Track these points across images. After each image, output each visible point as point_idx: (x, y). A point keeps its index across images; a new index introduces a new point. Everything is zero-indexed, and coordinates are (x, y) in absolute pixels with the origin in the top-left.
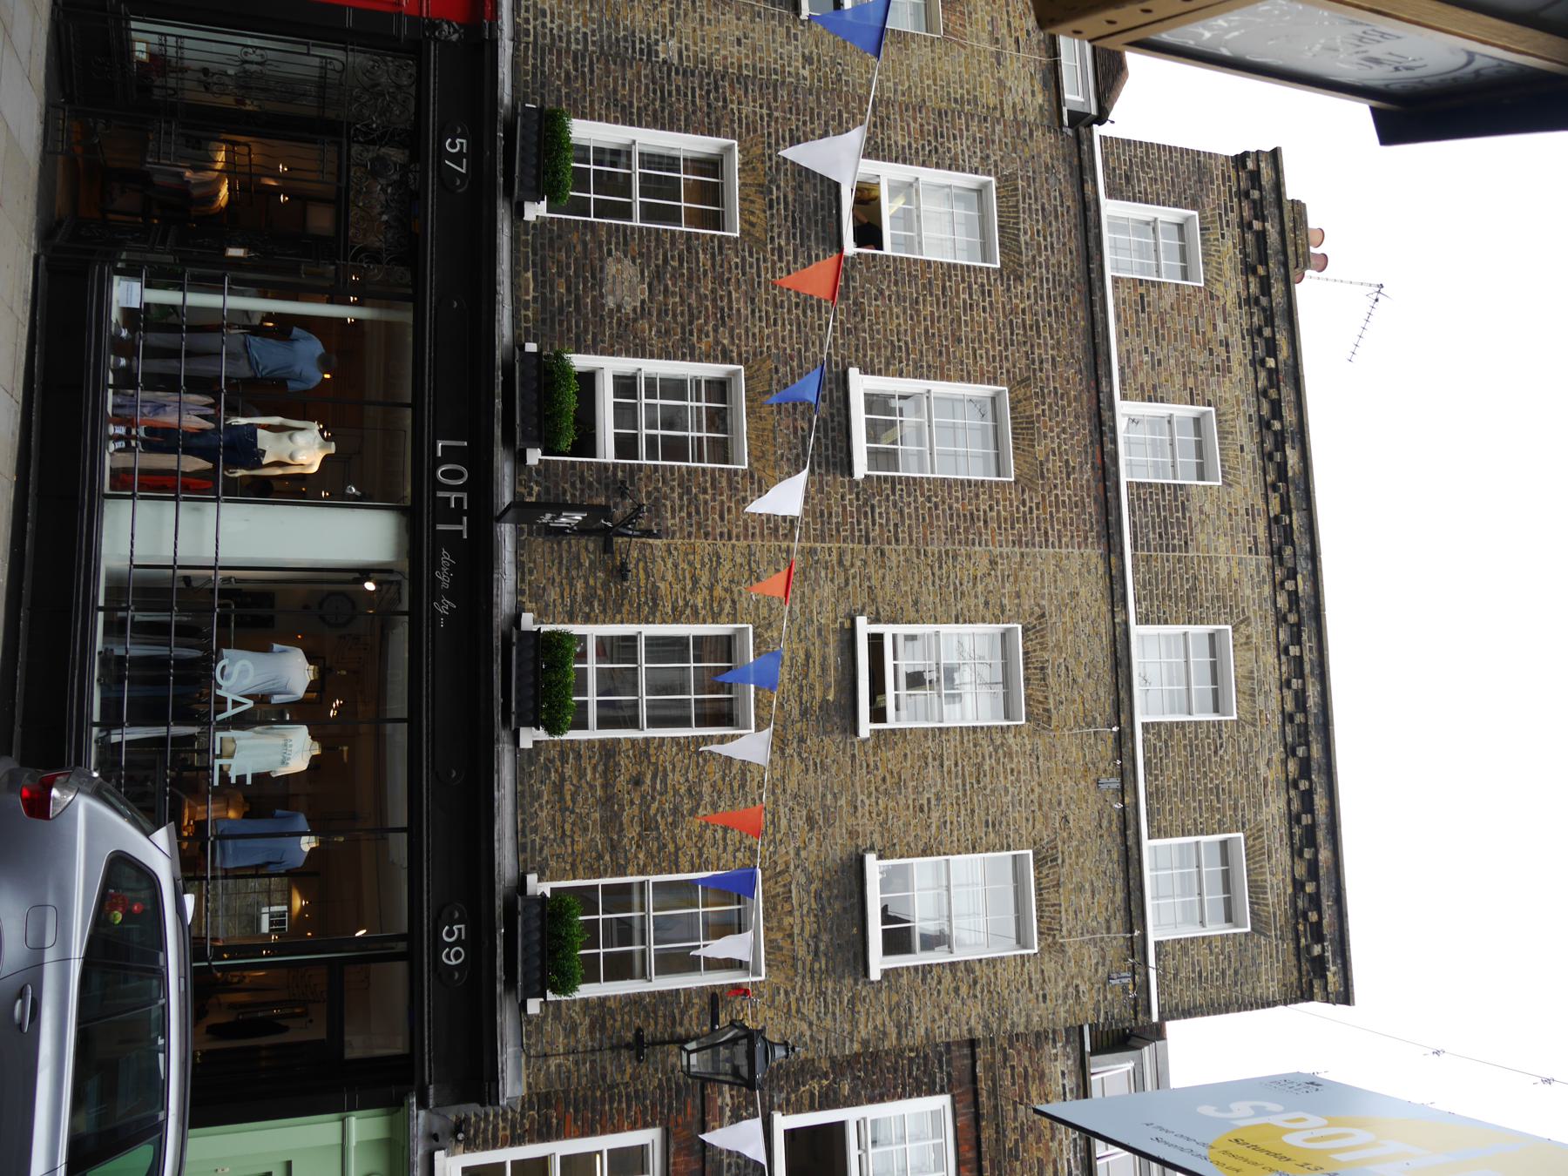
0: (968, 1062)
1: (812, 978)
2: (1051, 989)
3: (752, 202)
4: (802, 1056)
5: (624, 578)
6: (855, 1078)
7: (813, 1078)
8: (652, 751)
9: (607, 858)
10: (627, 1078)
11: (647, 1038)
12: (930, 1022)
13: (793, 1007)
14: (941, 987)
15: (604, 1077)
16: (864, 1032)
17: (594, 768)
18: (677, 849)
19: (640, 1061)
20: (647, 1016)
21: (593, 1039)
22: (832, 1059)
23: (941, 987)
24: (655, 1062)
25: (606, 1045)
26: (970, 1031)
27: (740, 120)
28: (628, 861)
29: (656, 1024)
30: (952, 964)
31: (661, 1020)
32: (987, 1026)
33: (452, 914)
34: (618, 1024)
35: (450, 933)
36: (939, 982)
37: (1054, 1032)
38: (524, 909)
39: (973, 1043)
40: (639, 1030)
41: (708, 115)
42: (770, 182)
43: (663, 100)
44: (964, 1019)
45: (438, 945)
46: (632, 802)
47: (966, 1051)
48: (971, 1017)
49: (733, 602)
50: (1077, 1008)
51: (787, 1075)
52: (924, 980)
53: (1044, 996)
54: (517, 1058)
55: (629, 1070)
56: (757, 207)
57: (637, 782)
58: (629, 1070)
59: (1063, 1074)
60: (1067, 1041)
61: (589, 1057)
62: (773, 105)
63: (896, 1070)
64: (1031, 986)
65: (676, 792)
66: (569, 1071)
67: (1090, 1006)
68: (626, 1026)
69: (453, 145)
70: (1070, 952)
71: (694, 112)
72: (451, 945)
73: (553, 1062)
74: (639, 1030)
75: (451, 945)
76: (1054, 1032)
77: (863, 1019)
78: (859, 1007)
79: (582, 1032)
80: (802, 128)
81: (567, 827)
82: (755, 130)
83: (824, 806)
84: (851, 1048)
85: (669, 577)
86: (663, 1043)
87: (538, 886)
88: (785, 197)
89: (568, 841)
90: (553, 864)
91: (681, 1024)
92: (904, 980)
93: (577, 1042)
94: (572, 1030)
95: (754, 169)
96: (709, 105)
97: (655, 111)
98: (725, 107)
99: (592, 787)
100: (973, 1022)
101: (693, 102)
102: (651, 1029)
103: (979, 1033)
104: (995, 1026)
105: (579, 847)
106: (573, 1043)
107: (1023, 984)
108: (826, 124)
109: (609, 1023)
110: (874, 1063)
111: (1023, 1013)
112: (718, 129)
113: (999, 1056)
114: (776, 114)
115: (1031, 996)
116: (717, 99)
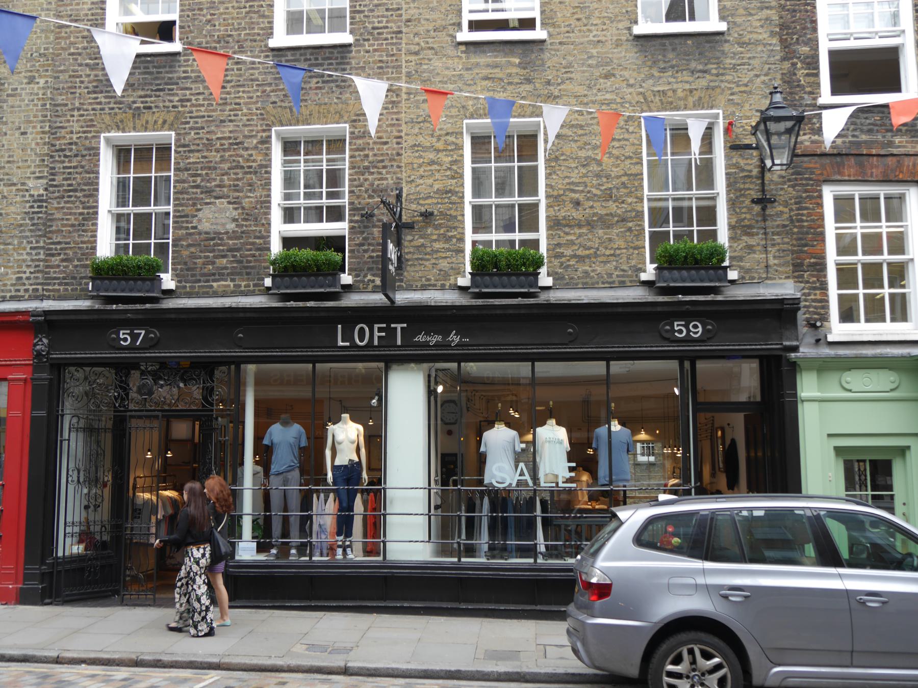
1: (723, 75)
3: (147, 122)
5: (431, 214)
7: (795, 74)
8: (555, 193)
9: (630, 224)
10: (786, 210)
11: (756, 195)
13: (743, 89)
15: (784, 226)
17: (567, 234)
18: (626, 174)
19: (775, 201)
20: (743, 195)
21: (757, 234)
22: (784, 59)
24: (776, 190)
25: (762, 224)
27: (84, 132)
28: (634, 210)
29: (750, 189)
31: (747, 186)
33: (667, 331)
34: (748, 216)
35: (680, 332)
38: (665, 281)
40: (753, 201)
41: (83, 156)
42: (130, 108)
43: (75, 190)
45: (688, 340)
46: (592, 207)
49: (447, 134)
51: (791, 93)
54: (767, 286)
55: (781, 208)
56: (151, 119)
57: (577, 203)
58: (781, 208)
61: (770, 236)
62: (70, 106)
65: (585, 176)
66: (779, 250)
68: (750, 210)
69: (125, 340)
71: (83, 167)
72: (689, 331)
73: (772, 261)
74: (753, 201)
75: (689, 331)
79: (752, 241)
80: (86, 84)
81: (608, 252)
82: (92, 120)
83: (597, 66)
85: (430, 181)
86: (763, 184)
87: (649, 272)
88: (141, 97)
89: (618, 252)
90: (633, 263)
91: (751, 171)
93: (758, 245)
94: (750, 248)
95: (122, 121)
96: (76, 156)
97: (85, 196)
98: (76, 144)
99: (580, 235)
101: (75, 167)
102: (752, 192)
105: (622, 244)
106: (759, 248)
108: (80, 65)
109: (747, 222)
112: (93, 148)
114: (77, 105)
116: (71, 150)
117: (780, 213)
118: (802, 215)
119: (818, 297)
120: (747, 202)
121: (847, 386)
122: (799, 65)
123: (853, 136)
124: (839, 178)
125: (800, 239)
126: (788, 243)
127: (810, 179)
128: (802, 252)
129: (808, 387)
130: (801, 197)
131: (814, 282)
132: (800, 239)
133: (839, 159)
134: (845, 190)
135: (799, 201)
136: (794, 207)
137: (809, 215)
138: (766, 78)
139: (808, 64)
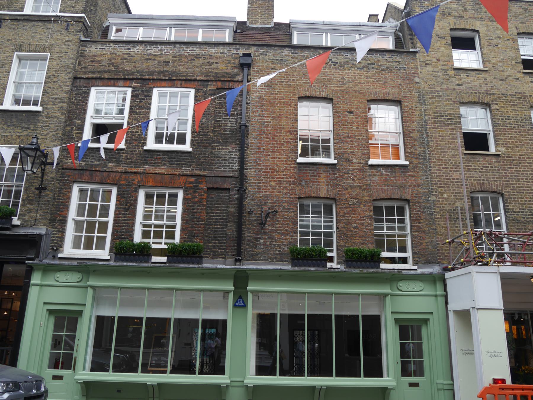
0: (82, 80)
1: (36, 130)
2: (63, 51)
4: (61, 135)
6: (76, 118)
12: (62, 92)
13: (43, 137)
14: (52, 87)
15: (48, 201)
16: (58, 114)
19: (46, 189)
23: (52, 87)
25: (38, 199)
26: (69, 78)
30: (45, 83)
31: (35, 181)
32: (69, 73)
36: (50, 88)
37: (81, 50)
39: (75, 78)
40: (36, 188)
44: (65, 80)
47: (78, 81)
48: (65, 79)
50: (73, 42)
52: (47, 93)
53: (66, 52)
54: (34, 229)
58: (48, 193)
59: (96, 49)
60: (86, 46)
61: (40, 205)
63: (77, 105)
64: (61, 57)
67: (74, 37)
68: (34, 192)
70: (53, 42)
73: (39, 217)
74: (36, 188)
76: (81, 50)
77: (54, 114)
78: (50, 115)
84: (63, 119)
86: (42, 181)
91: (38, 174)
92: (46, 99)
100: (66, 77)
102: (37, 184)
103: (71, 75)
104: (70, 70)
106: (34, 210)
107: (59, 59)
110: (73, 112)
111: (69, 60)
113: (84, 70)
115: (64, 57)
117: (48, 195)
118: (60, 196)
119: (60, 236)
120: (33, 189)
121: (57, 279)
122: (75, 128)
123: (91, 162)
124: (80, 180)
125: (57, 208)
126: (48, 209)
127: (67, 180)
128: (57, 214)
129: (36, 279)
130: (61, 188)
131: (59, 228)
132: (57, 208)
133: (82, 172)
134: (84, 186)
135: (60, 190)
136: (57, 193)
137: (63, 196)
138: (55, 133)
139: (79, 128)
